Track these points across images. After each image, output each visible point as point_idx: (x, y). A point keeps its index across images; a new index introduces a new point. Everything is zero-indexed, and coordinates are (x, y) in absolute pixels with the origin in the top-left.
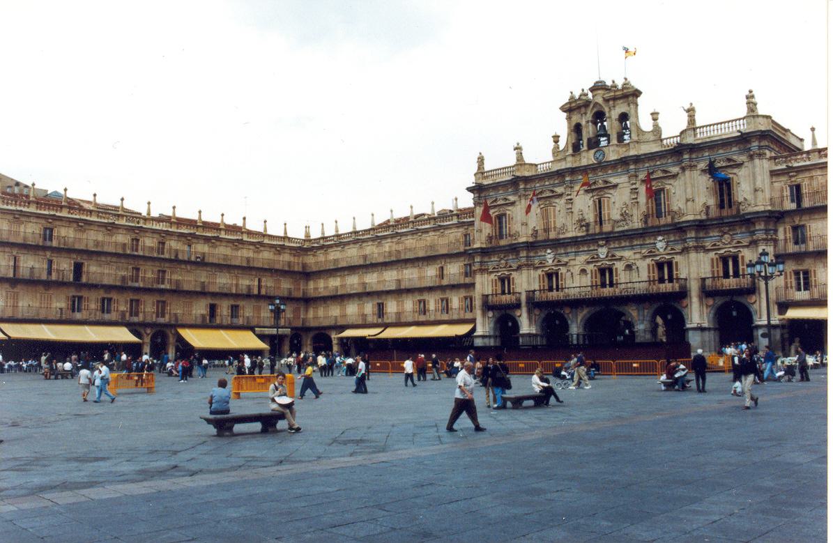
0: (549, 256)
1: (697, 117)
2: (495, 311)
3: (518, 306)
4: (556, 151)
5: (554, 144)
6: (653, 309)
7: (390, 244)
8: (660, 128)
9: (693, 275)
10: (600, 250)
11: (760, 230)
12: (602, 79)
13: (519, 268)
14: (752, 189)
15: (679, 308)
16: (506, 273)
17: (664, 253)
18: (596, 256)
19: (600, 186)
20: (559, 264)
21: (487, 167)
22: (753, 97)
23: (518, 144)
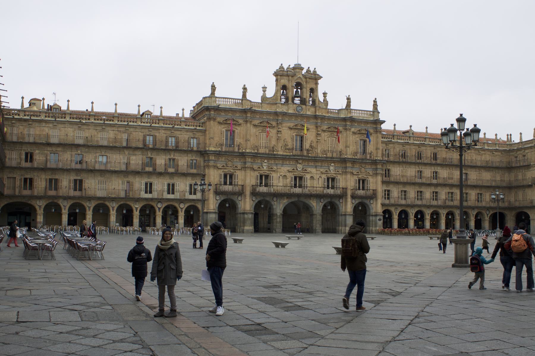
0: (265, 164)
1: (351, 104)
2: (221, 196)
3: (241, 193)
4: (264, 98)
5: (263, 92)
6: (323, 204)
7: (117, 132)
8: (328, 102)
9: (349, 187)
10: (298, 165)
11: (380, 169)
12: (299, 63)
13: (244, 168)
14: (375, 148)
15: (338, 203)
16: (232, 171)
17: (333, 173)
18: (295, 169)
19: (299, 128)
20: (271, 169)
21: (217, 94)
22: (376, 102)
23: (245, 85)
